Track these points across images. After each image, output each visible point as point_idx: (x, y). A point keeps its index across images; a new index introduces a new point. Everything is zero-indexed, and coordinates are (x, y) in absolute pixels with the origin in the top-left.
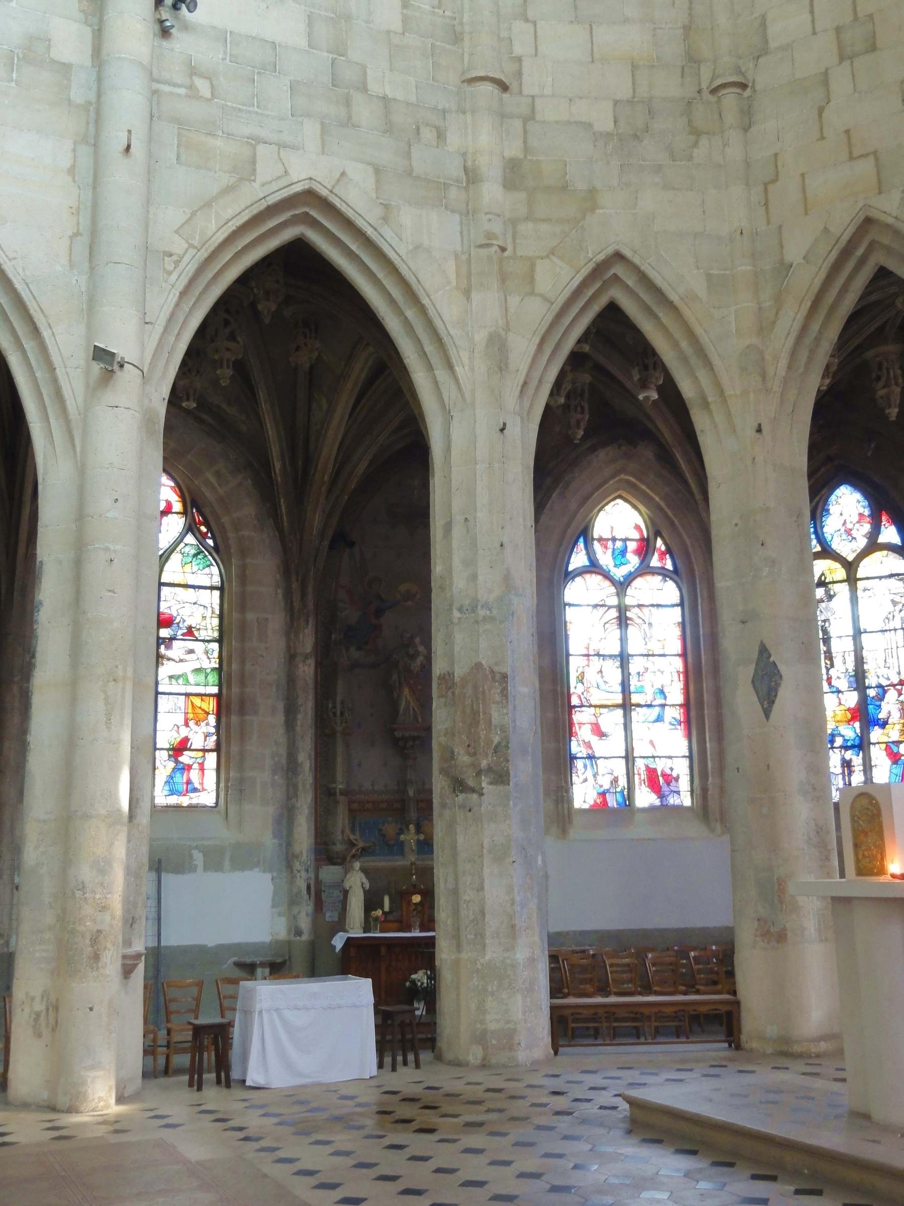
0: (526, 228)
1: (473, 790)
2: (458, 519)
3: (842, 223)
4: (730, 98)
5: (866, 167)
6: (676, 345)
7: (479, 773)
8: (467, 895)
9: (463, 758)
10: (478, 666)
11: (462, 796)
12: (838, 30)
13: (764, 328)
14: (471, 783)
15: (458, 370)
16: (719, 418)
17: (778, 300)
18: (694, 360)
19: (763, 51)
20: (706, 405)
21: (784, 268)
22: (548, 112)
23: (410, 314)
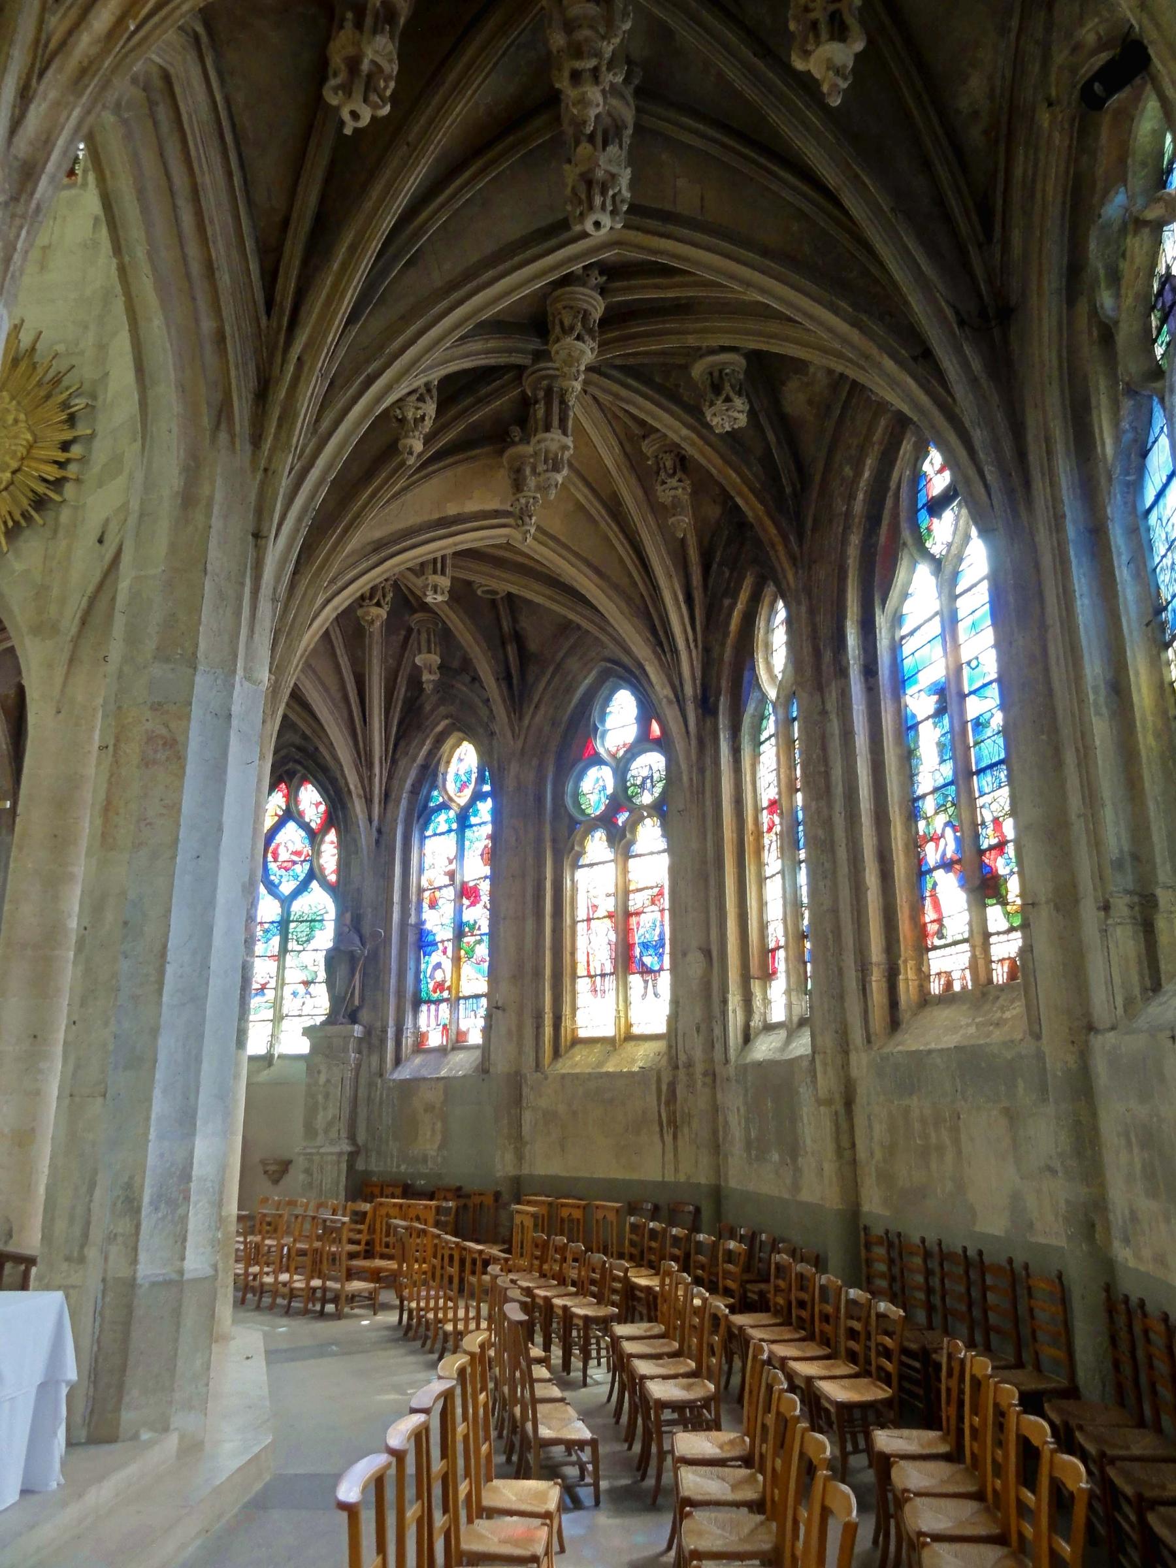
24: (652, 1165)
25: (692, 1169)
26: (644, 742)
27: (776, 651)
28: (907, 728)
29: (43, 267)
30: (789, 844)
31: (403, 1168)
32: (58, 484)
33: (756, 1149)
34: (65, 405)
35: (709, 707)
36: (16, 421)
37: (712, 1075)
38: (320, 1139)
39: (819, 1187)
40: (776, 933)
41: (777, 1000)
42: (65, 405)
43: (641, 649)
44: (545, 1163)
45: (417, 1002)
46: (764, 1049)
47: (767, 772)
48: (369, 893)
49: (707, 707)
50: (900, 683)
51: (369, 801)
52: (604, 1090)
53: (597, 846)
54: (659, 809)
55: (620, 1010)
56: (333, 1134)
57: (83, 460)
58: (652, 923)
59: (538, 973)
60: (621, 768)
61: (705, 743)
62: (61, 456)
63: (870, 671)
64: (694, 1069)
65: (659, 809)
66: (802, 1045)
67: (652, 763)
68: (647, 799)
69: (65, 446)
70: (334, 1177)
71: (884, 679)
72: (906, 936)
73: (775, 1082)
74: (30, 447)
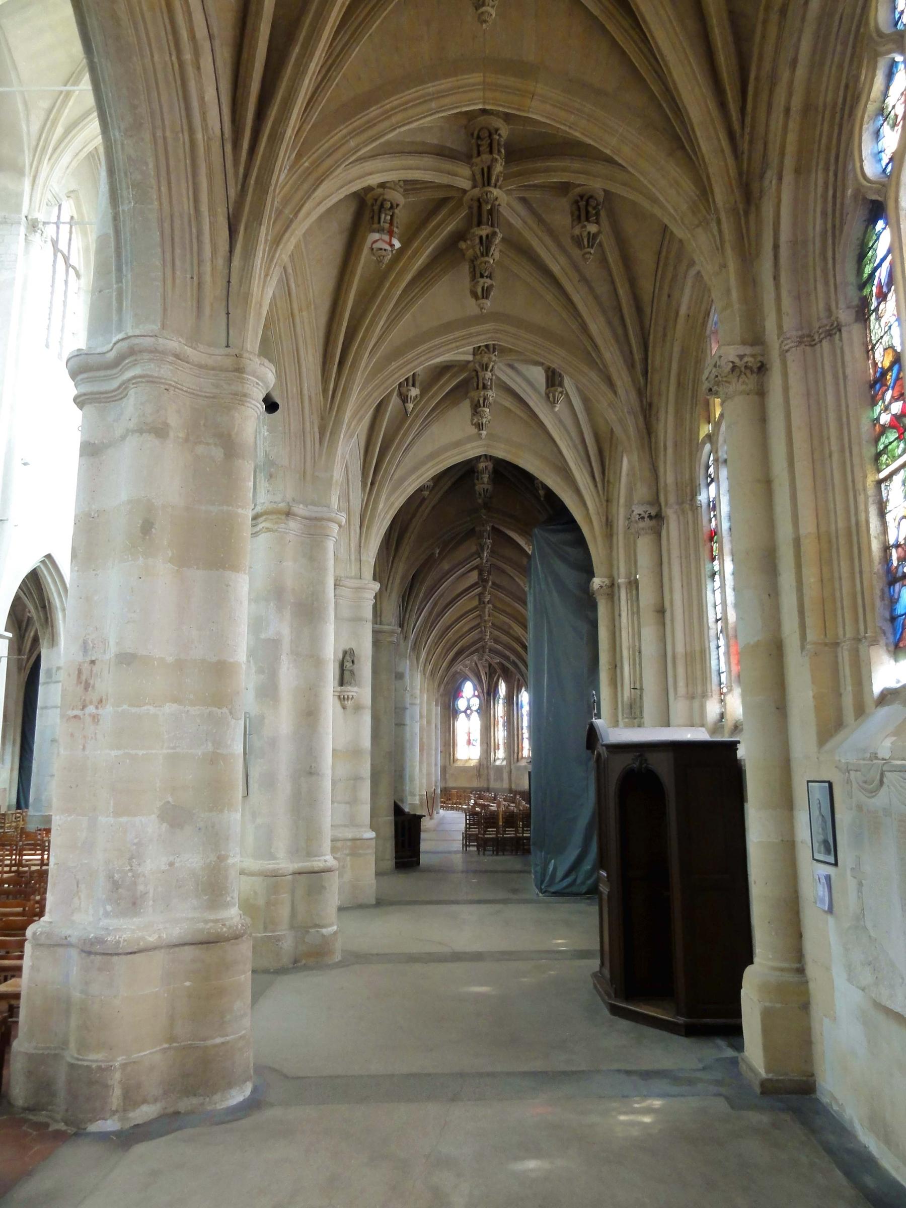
24: (475, 784)
25: (483, 784)
26: (474, 696)
27: (502, 688)
28: (522, 715)
30: (504, 726)
33: (496, 780)
35: (488, 694)
37: (487, 767)
39: (505, 785)
40: (501, 742)
41: (501, 754)
43: (476, 682)
44: (451, 784)
46: (498, 763)
47: (500, 709)
49: (489, 694)
50: (522, 707)
52: (465, 770)
53: (462, 716)
54: (477, 711)
55: (468, 752)
58: (476, 735)
59: (449, 745)
60: (469, 700)
61: (488, 702)
63: (517, 704)
64: (484, 766)
65: (477, 711)
66: (504, 763)
67: (475, 703)
68: (475, 708)
71: (519, 707)
72: (520, 749)
73: (499, 769)
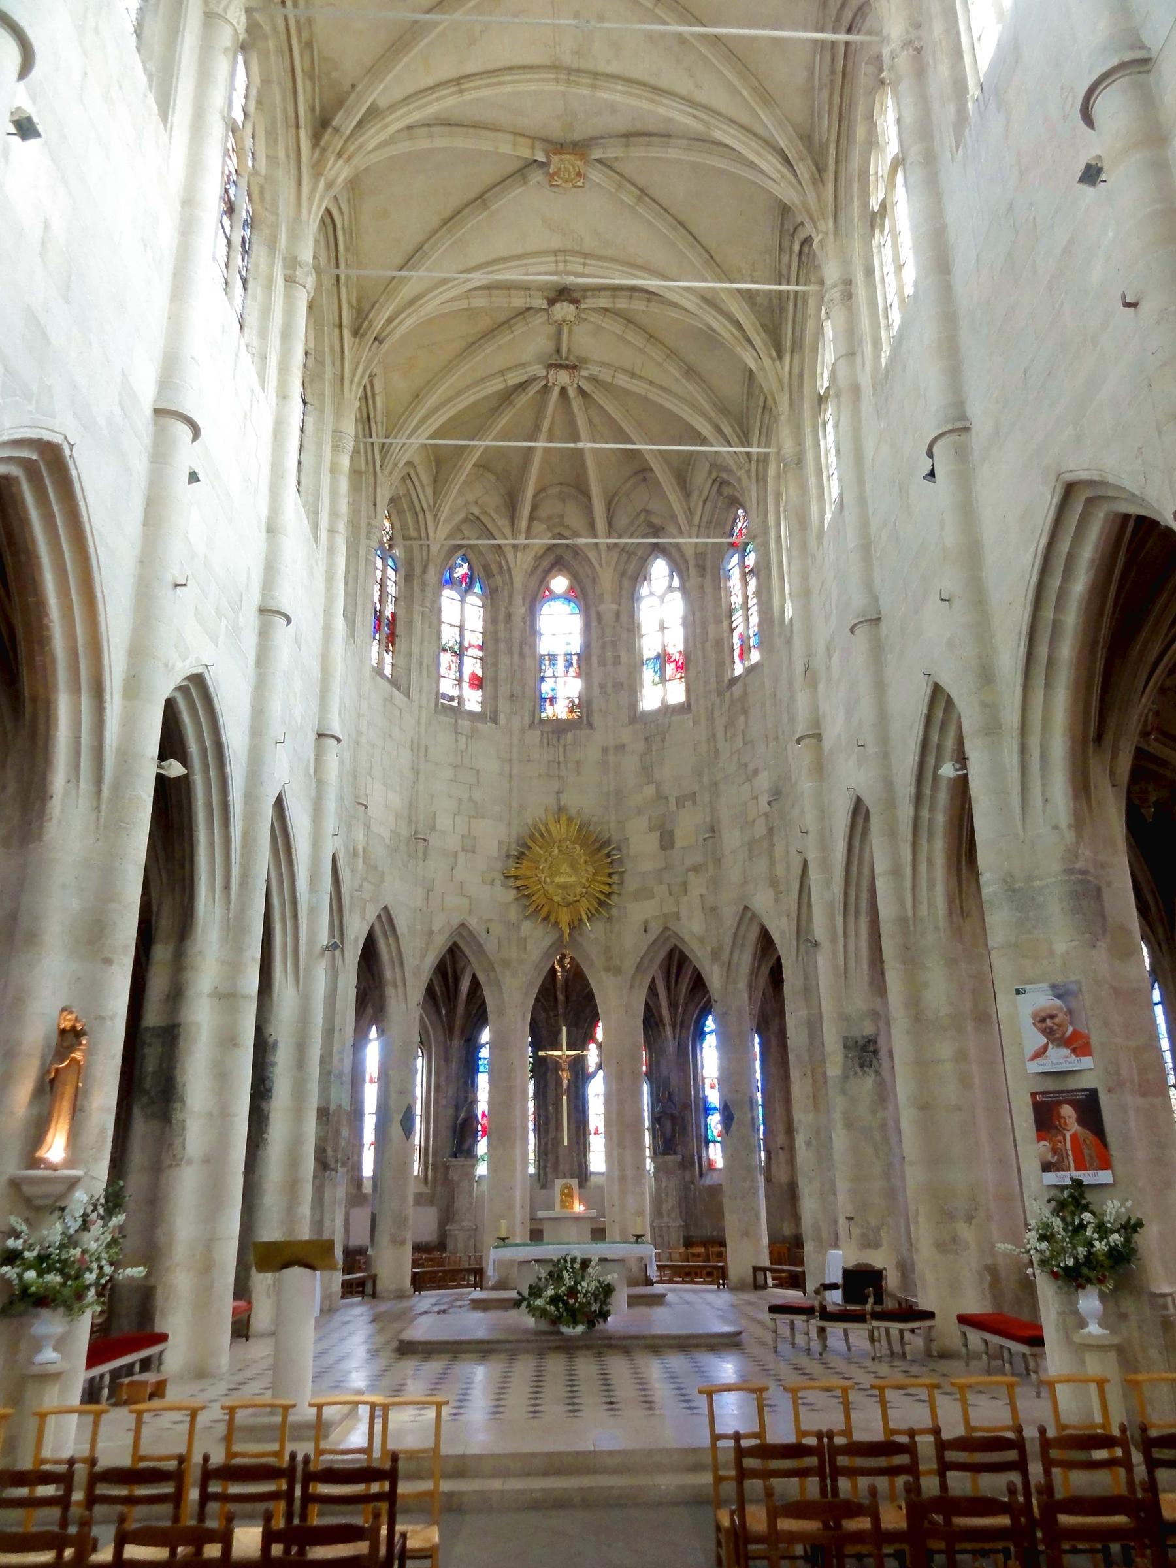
0: (365, 884)
1: (333, 1170)
2: (337, 1028)
3: (455, 923)
4: (421, 844)
5: (466, 901)
6: (390, 952)
7: (337, 1161)
8: (327, 1223)
9: (330, 1152)
10: (340, 1106)
11: (327, 1173)
12: (463, 836)
13: (423, 956)
14: (332, 1166)
15: (346, 953)
16: (400, 990)
17: (427, 945)
18: (397, 964)
19: (433, 828)
20: (395, 986)
21: (431, 933)
22: (375, 828)
23: (336, 918)
29: (578, 773)
31: (715, 1233)
32: (609, 895)
34: (608, 855)
36: (586, 862)
38: (666, 1219)
42: (608, 855)
45: (707, 1142)
48: (674, 1081)
51: (674, 1026)
56: (673, 1215)
57: (621, 883)
62: (610, 881)
69: (610, 875)
70: (676, 1237)
74: (594, 875)
